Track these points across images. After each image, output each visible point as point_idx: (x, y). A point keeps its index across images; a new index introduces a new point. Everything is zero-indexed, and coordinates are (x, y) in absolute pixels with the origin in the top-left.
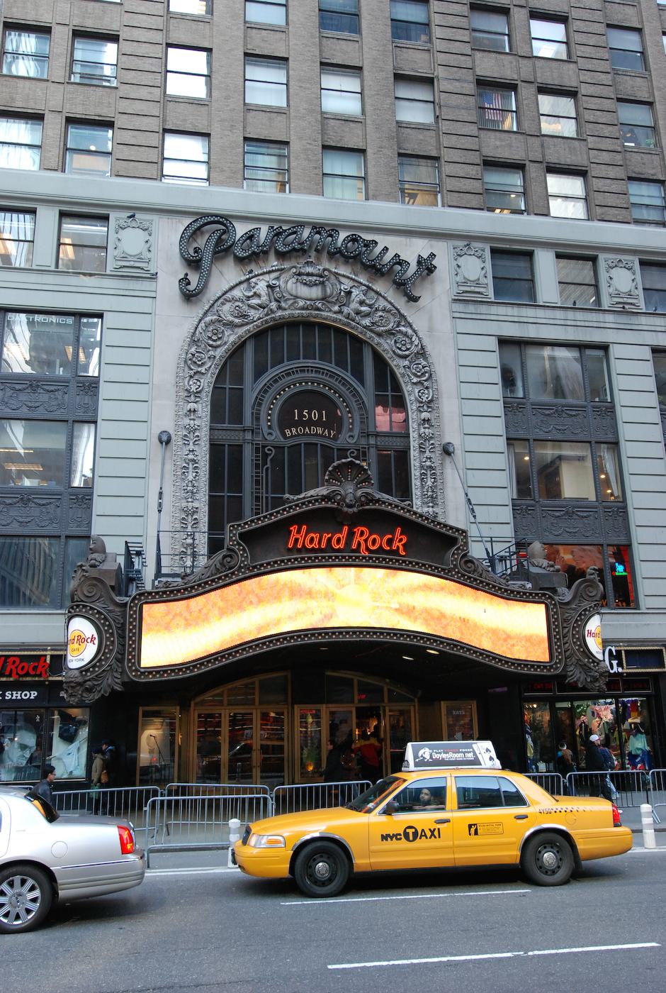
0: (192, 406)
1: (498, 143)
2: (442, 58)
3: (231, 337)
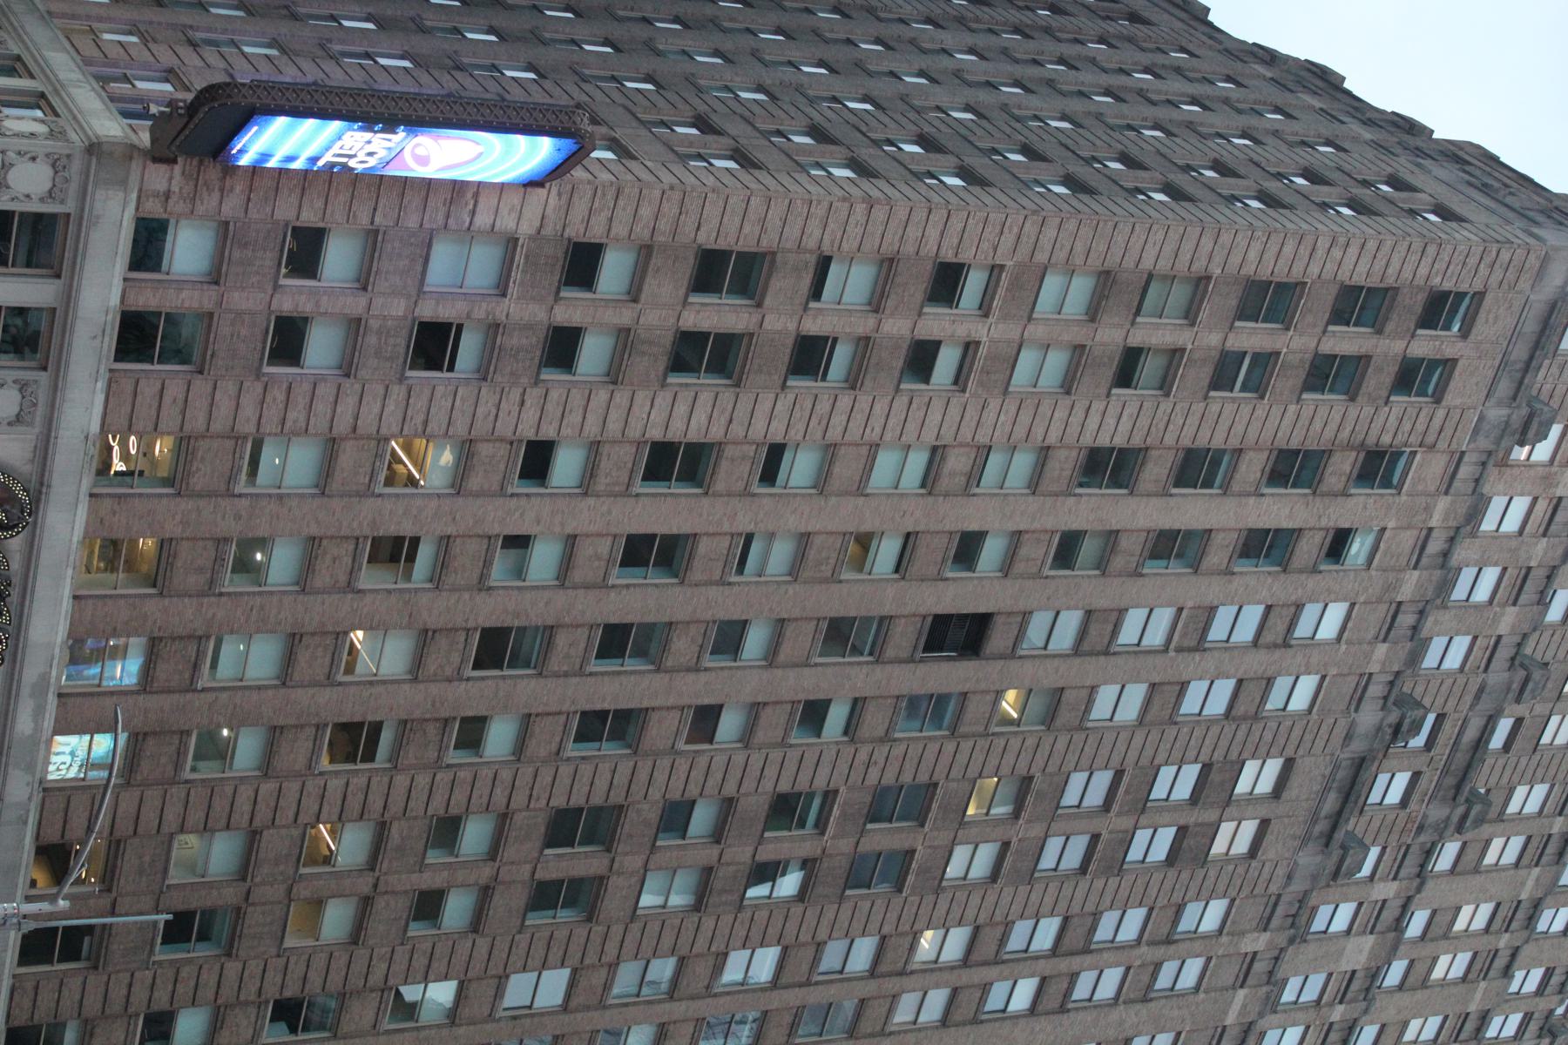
1: (147, 859)
2: (292, 788)
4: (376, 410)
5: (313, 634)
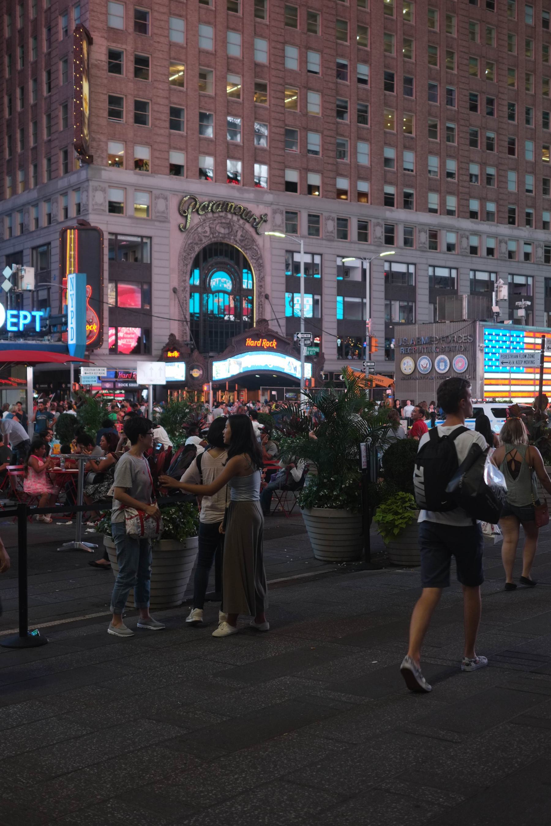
0: (184, 278)
1: (291, 159)
3: (197, 249)
4: (161, 91)
5: (228, 109)
